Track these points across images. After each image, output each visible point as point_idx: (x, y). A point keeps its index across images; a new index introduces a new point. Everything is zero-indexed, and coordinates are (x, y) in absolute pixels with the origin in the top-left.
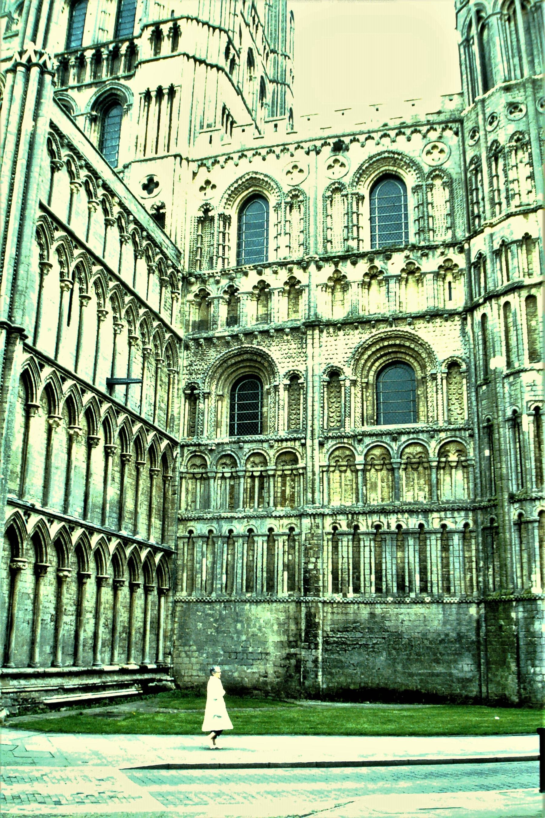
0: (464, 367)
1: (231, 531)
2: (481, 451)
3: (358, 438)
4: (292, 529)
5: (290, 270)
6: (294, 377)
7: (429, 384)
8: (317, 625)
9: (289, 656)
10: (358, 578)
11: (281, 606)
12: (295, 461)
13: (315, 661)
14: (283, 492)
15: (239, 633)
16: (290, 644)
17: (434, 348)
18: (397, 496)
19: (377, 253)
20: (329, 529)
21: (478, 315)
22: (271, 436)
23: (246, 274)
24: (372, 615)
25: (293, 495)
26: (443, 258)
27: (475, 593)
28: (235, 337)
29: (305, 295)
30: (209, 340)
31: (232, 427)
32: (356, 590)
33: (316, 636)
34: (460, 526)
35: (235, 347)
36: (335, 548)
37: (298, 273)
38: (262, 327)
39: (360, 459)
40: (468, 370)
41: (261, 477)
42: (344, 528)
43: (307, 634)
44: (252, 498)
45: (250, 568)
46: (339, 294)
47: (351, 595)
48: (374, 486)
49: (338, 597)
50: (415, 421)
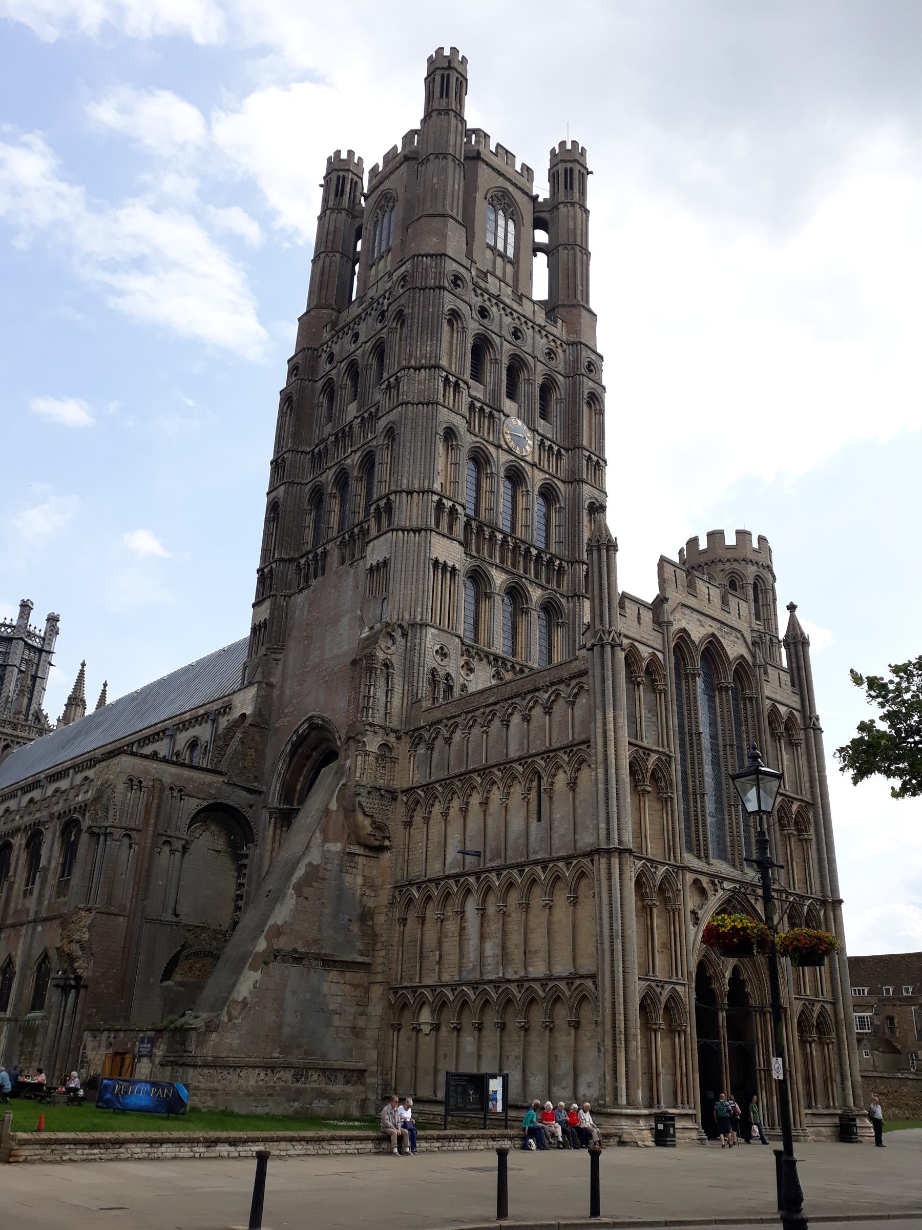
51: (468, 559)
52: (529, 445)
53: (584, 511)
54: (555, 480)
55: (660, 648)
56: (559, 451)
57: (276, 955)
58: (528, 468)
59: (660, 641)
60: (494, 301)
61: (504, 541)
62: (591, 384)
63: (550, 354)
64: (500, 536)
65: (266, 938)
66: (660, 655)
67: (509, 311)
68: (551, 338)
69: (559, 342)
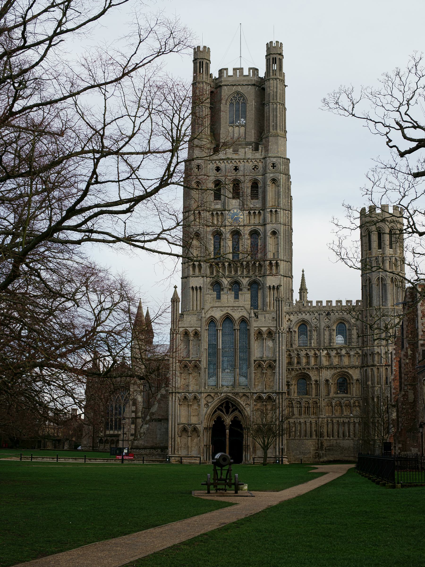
0: (360, 381)
1: (300, 421)
2: (364, 404)
3: (333, 398)
4: (316, 421)
5: (315, 351)
6: (316, 381)
7: (351, 385)
8: (323, 445)
9: (316, 453)
10: (333, 434)
11: (314, 440)
12: (317, 403)
13: (323, 454)
14: (313, 411)
15: (303, 447)
16: (316, 450)
17: (353, 376)
18: (343, 413)
19: (339, 348)
20: (326, 421)
21: (365, 369)
22: (310, 397)
23: (302, 351)
24: (337, 442)
25: (316, 412)
26: (355, 351)
27: (361, 438)
28: (300, 369)
29: (319, 358)
30: (292, 369)
31: (298, 392)
32: (333, 436)
33: (323, 448)
34: (358, 421)
35: (300, 372)
36: (327, 426)
37: (317, 352)
38: (307, 366)
39: (333, 404)
40: (361, 382)
41: (307, 407)
42: (330, 421)
43: (321, 447)
44: (305, 412)
45: (306, 431)
46: (328, 358)
47: (331, 438)
48: (337, 411)
49: (328, 438)
50: (347, 393)
51: (211, 279)
52: (242, 218)
53: (268, 237)
54: (257, 227)
55: (200, 326)
56: (259, 212)
57: (151, 420)
58: (241, 228)
59: (200, 324)
60: (221, 162)
61: (229, 265)
62: (271, 175)
63: (255, 167)
64: (227, 264)
65: (149, 416)
66: (199, 329)
67: (229, 161)
68: (253, 161)
69: (258, 161)
